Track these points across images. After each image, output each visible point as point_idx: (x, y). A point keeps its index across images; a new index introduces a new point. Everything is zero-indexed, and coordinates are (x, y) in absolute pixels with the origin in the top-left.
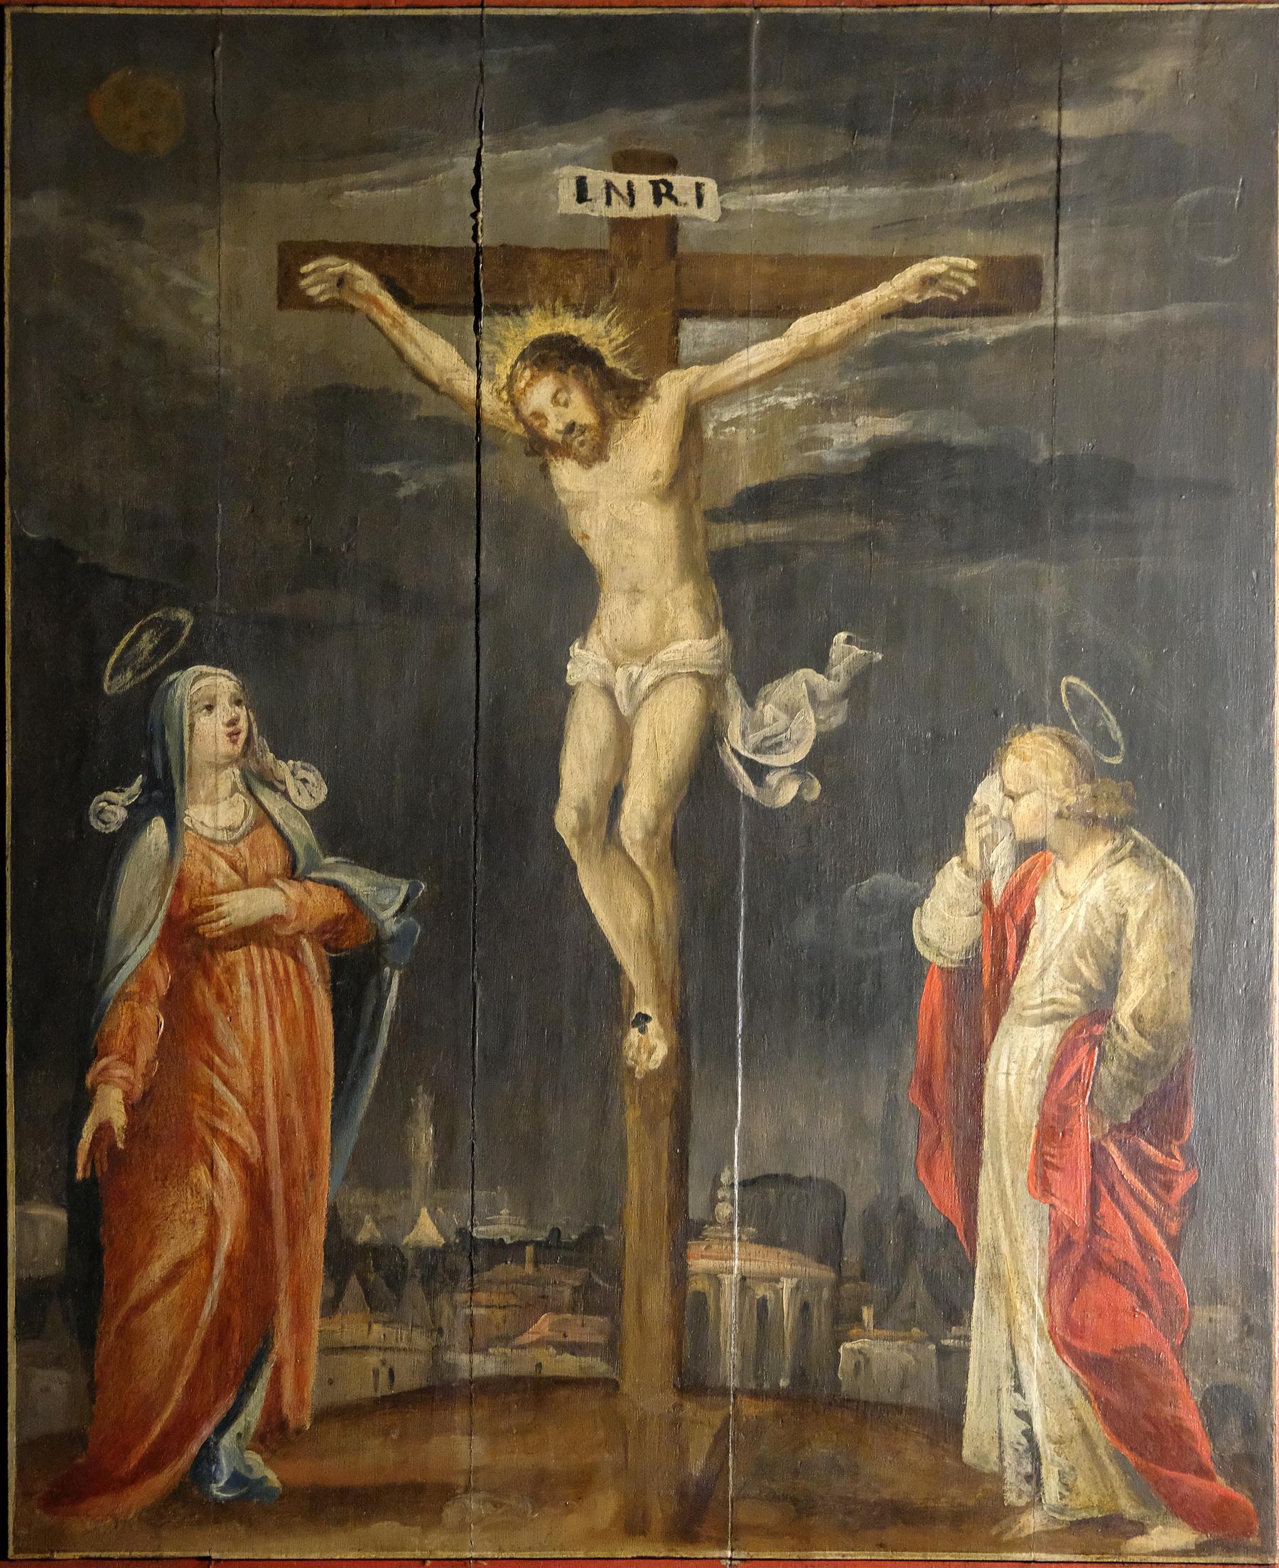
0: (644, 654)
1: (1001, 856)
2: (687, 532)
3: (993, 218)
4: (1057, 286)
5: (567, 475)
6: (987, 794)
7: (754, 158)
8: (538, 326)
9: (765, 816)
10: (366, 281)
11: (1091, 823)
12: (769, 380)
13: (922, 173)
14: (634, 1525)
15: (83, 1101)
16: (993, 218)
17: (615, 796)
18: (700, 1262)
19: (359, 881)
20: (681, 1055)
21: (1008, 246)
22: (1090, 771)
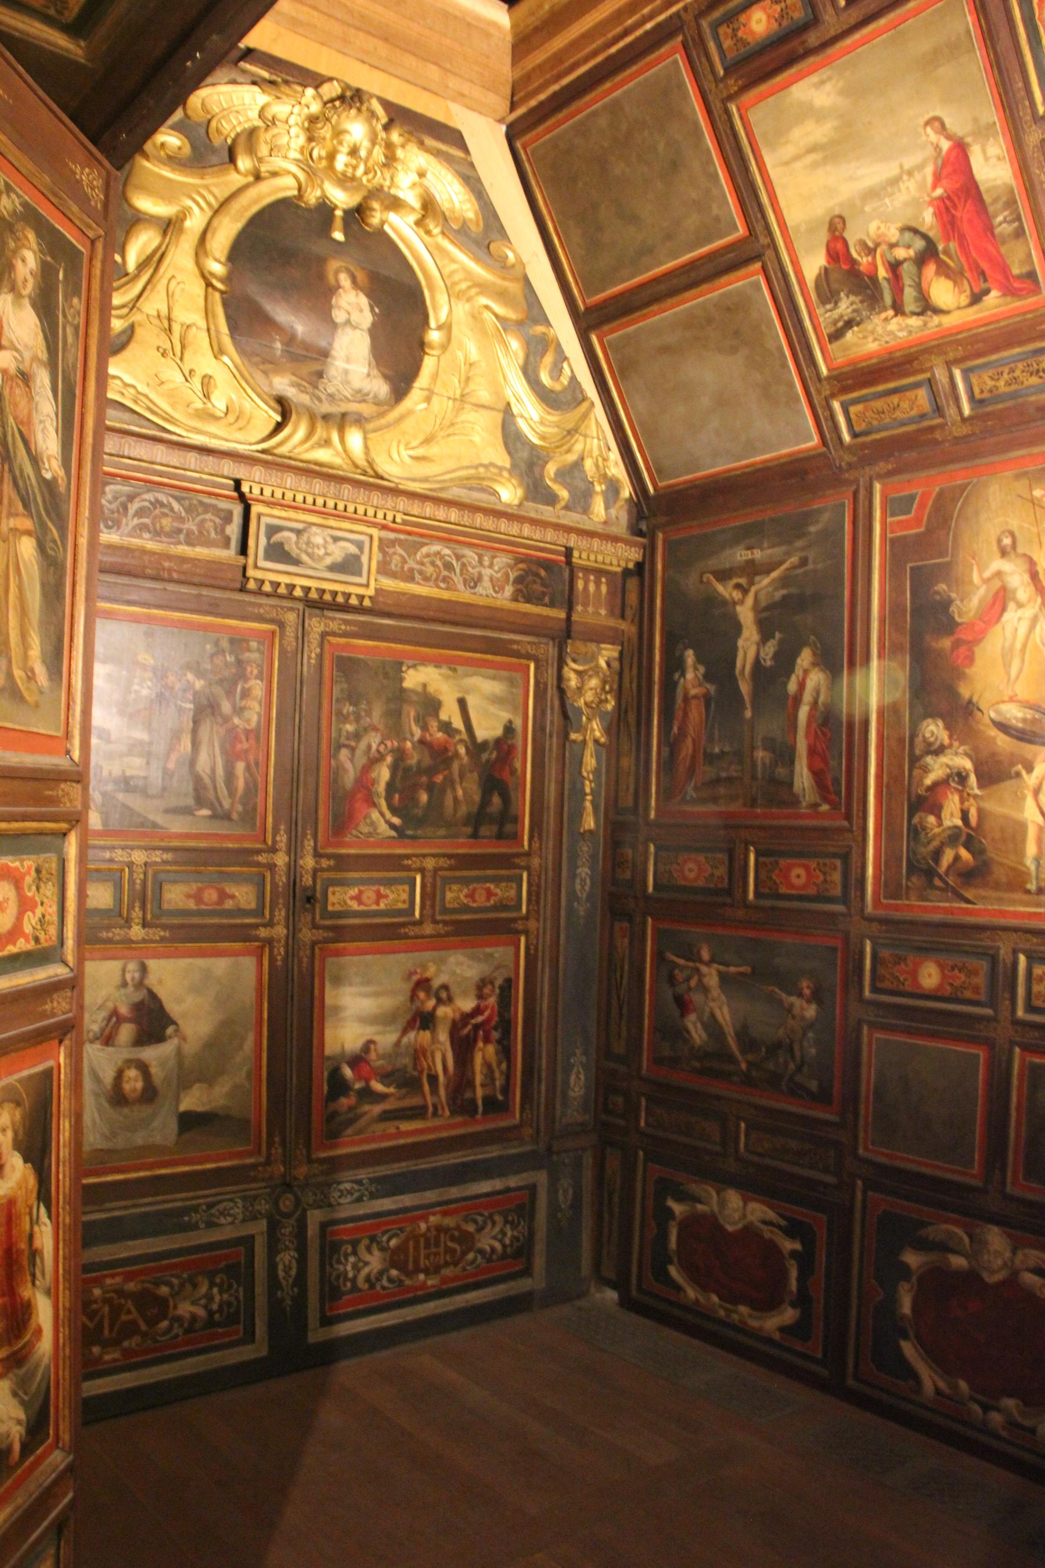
0: (747, 639)
1: (801, 673)
2: (756, 616)
3: (803, 549)
4: (810, 561)
5: (739, 608)
6: (799, 661)
7: (766, 545)
8: (735, 581)
9: (765, 668)
10: (711, 577)
11: (814, 664)
12: (766, 587)
13: (790, 543)
14: (745, 805)
15: (671, 728)
16: (803, 549)
17: (744, 667)
18: (755, 754)
19: (708, 686)
20: (753, 717)
21: (803, 554)
22: (814, 654)
